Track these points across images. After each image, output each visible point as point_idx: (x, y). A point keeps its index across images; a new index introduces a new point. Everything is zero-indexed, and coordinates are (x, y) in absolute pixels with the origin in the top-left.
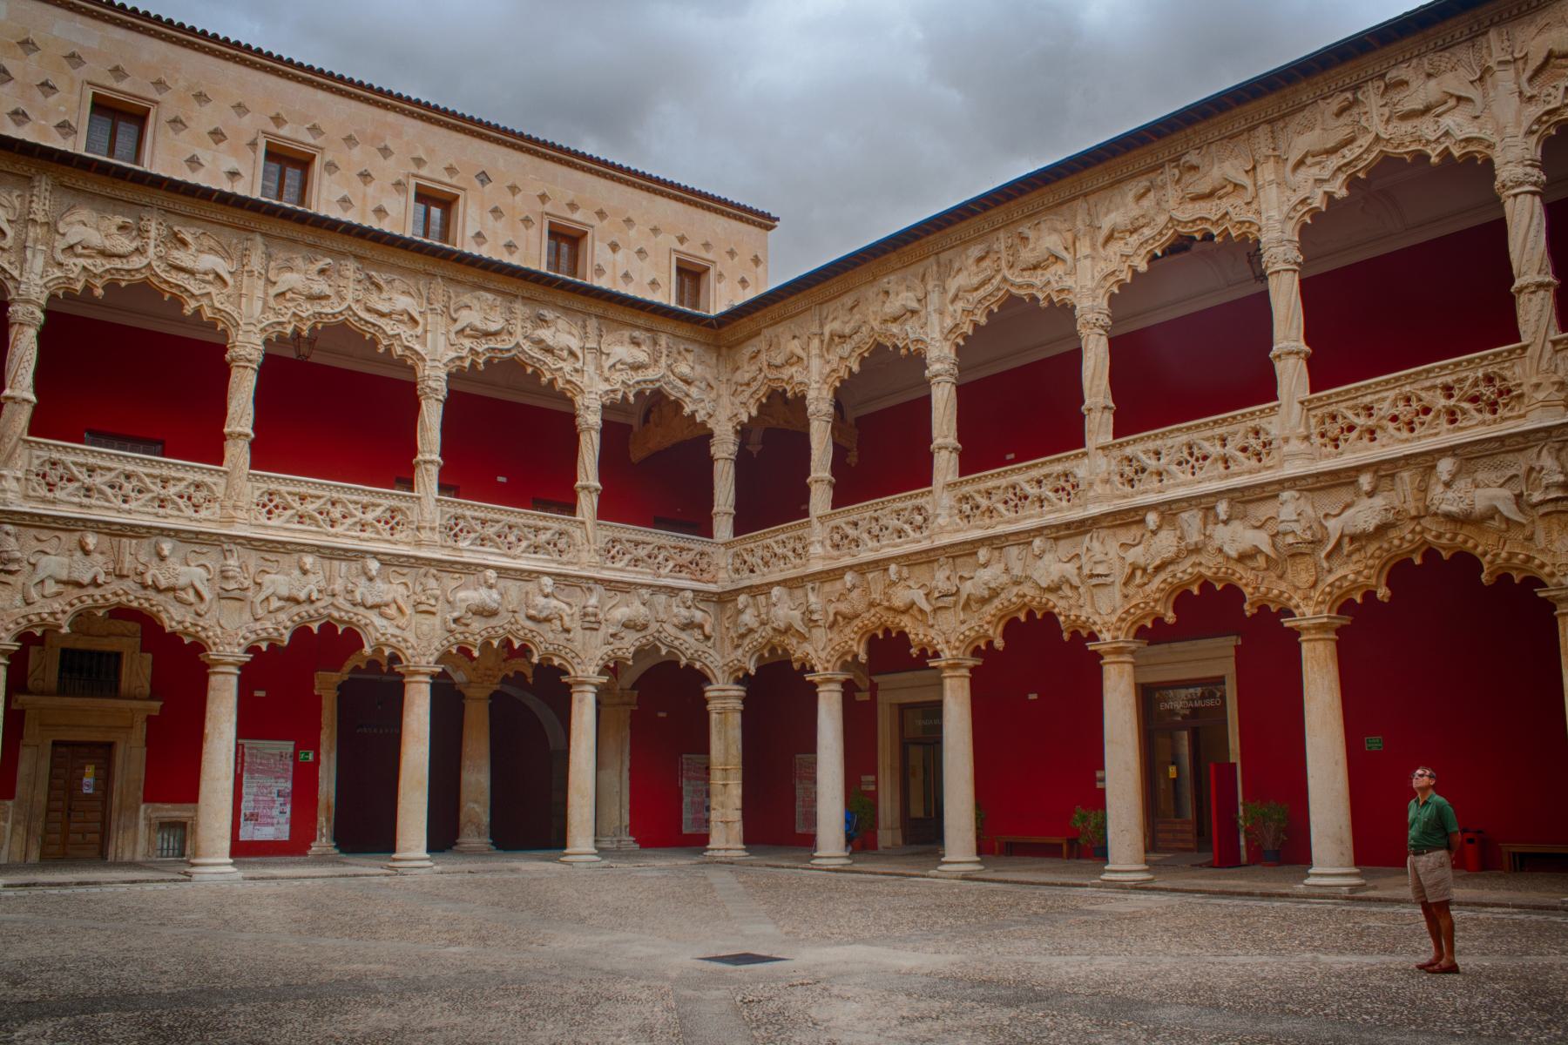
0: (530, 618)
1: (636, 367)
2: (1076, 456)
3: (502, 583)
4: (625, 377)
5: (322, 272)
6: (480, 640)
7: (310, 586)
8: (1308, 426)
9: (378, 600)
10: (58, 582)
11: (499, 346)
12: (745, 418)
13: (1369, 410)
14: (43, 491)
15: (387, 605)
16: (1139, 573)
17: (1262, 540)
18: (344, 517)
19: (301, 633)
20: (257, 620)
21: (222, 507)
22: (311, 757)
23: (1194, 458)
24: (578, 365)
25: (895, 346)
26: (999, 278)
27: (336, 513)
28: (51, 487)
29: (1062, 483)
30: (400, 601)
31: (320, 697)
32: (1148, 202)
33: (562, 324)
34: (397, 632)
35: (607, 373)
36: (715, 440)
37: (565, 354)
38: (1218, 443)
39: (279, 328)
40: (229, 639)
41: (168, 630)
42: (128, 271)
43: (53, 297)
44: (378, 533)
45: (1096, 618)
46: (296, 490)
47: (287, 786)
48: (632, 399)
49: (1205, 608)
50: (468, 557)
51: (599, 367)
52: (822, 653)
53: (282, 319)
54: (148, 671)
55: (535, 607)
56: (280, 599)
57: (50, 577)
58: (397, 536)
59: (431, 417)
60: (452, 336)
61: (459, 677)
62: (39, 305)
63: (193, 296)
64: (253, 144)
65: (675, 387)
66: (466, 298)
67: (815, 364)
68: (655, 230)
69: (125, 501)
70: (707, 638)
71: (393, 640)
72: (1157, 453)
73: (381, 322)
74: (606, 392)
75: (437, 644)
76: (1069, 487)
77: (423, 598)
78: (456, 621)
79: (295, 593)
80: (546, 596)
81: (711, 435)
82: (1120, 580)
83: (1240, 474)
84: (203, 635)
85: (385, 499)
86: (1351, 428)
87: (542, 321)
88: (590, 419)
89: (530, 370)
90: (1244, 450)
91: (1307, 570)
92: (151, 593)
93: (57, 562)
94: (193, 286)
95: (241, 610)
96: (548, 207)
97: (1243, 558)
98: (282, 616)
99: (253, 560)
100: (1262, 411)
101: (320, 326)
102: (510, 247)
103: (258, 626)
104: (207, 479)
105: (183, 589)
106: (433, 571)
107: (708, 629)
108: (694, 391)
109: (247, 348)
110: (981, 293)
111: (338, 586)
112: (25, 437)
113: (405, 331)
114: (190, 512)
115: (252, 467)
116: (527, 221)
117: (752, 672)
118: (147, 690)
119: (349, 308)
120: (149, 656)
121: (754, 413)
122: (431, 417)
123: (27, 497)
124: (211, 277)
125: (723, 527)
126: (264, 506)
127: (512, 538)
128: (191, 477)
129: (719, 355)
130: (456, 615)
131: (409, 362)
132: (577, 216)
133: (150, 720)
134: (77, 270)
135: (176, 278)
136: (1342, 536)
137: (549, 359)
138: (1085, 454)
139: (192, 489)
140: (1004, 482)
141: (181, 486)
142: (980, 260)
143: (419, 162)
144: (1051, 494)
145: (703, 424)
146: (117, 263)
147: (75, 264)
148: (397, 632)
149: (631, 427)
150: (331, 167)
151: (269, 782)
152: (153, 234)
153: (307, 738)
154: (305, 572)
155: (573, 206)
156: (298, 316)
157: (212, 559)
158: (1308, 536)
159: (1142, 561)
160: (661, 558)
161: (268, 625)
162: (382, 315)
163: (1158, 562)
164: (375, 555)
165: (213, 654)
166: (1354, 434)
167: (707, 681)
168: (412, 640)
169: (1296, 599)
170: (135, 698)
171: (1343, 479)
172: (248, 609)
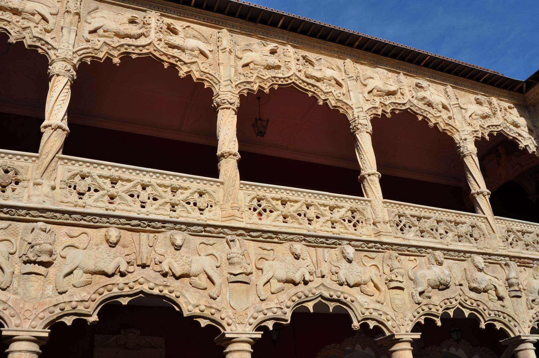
0: (472, 289)
3: (446, 262)
4: (480, 123)
5: (273, 52)
6: (440, 312)
18: (318, 217)
21: (222, 209)
24: (450, 114)
27: (311, 213)
30: (375, 280)
34: (378, 306)
37: (440, 107)
39: (248, 86)
41: (186, 314)
42: (137, 47)
44: (346, 228)
46: (278, 196)
48: (487, 138)
51: (464, 117)
53: (249, 80)
55: (475, 280)
56: (279, 281)
60: (366, 95)
63: (185, 63)
65: (511, 130)
69: (143, 207)
71: (375, 315)
73: (318, 84)
75: (410, 315)
77: (393, 277)
78: (421, 293)
80: (480, 270)
84: (217, 317)
85: (346, 203)
88: (469, 148)
89: (420, 118)
92: (170, 280)
94: (185, 57)
95: (248, 291)
98: (283, 297)
99: (253, 248)
101: (276, 87)
103: (264, 306)
106: (395, 254)
111: (325, 269)
115: (241, 179)
124: (197, 53)
126: (255, 210)
129: (529, 112)
130: (420, 289)
131: (341, 111)
134: (100, 44)
135: (171, 52)
139: (196, 195)
141: (187, 193)
148: (378, 306)
152: (153, 25)
154: (297, 257)
156: (261, 80)
157: (220, 248)
161: (272, 305)
162: (318, 80)
172: (253, 291)
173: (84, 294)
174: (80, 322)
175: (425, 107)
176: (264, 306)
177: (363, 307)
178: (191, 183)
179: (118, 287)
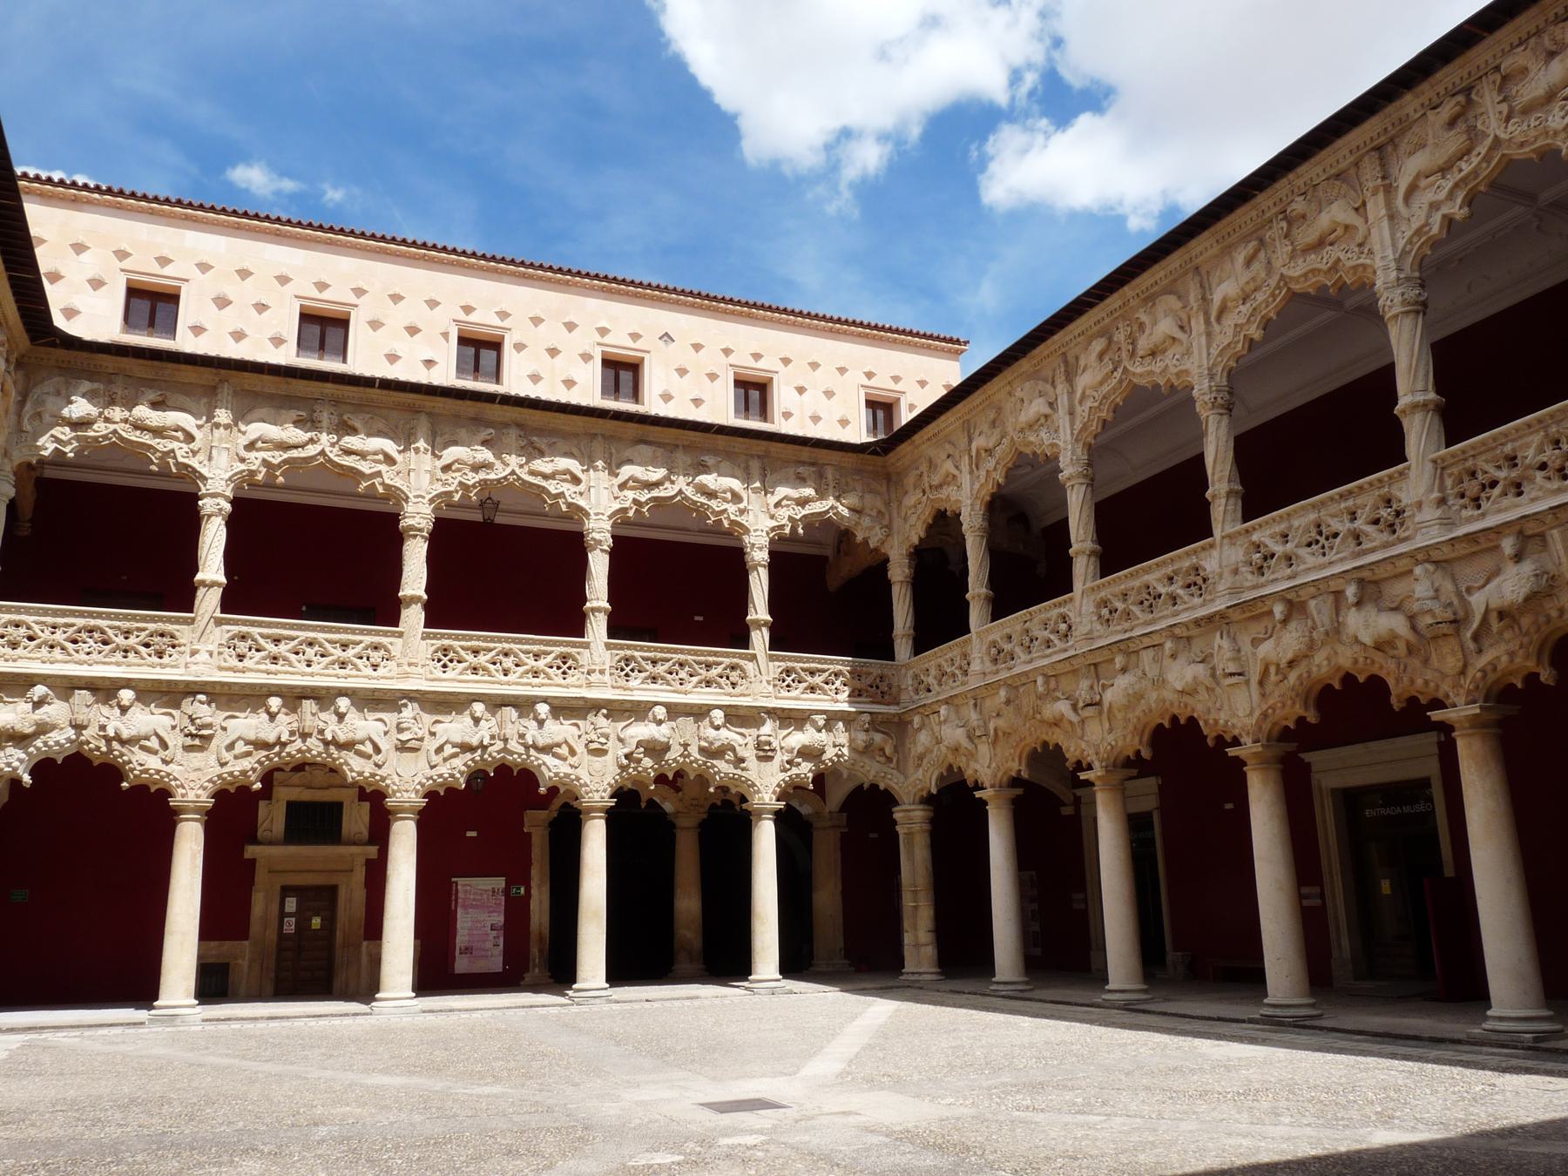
1: (803, 502)
2: (1203, 549)
4: (791, 513)
7: (483, 733)
8: (1442, 488)
9: (549, 741)
10: (248, 743)
11: (662, 494)
12: (916, 541)
13: (1512, 460)
14: (234, 662)
15: (559, 745)
16: (1272, 670)
17: (1396, 624)
19: (476, 775)
20: (432, 767)
21: (399, 665)
22: (522, 890)
23: (1321, 538)
25: (1035, 453)
26: (1120, 370)
27: (508, 662)
28: (241, 657)
29: (1192, 578)
31: (529, 834)
32: (1257, 266)
33: (726, 465)
36: (890, 565)
37: (729, 495)
38: (1346, 517)
40: (407, 786)
43: (237, 488)
45: (1235, 721)
47: (499, 919)
49: (1353, 707)
50: (638, 696)
52: (989, 768)
54: (367, 819)
57: (240, 738)
58: (569, 680)
59: (599, 566)
61: (668, 807)
64: (445, 335)
66: (628, 453)
67: (965, 479)
68: (842, 370)
70: (889, 760)
72: (1285, 537)
74: (773, 529)
76: (1200, 581)
77: (594, 737)
78: (627, 756)
79: (467, 739)
80: (717, 728)
81: (887, 560)
82: (1254, 679)
83: (1373, 550)
85: (556, 645)
86: (1494, 484)
87: (704, 469)
88: (759, 556)
90: (1376, 522)
91: (1453, 653)
93: (249, 724)
94: (365, 467)
96: (732, 359)
97: (1379, 646)
100: (1390, 477)
102: (697, 402)
104: (384, 640)
105: (362, 743)
107: (888, 751)
108: (866, 522)
109: (418, 516)
110: (1106, 388)
112: (218, 614)
113: (567, 489)
114: (369, 671)
116: (713, 377)
117: (934, 791)
118: (365, 834)
119: (513, 472)
121: (923, 535)
123: (221, 669)
124: (381, 457)
125: (903, 648)
128: (368, 639)
130: (626, 751)
132: (761, 364)
134: (257, 463)
136: (1487, 611)
137: (713, 503)
138: (1212, 546)
140: (1137, 583)
141: (359, 649)
142: (1101, 356)
143: (603, 331)
144: (1180, 592)
145: (876, 550)
146: (294, 453)
147: (256, 458)
148: (569, 770)
149: (826, 558)
150: (519, 347)
151: (483, 916)
152: (325, 423)
153: (518, 874)
155: (757, 356)
158: (1449, 615)
159: (1273, 657)
160: (838, 683)
162: (546, 477)
163: (1290, 656)
164: (545, 700)
165: (390, 802)
166: (1497, 491)
167: (897, 804)
168: (585, 778)
169: (1445, 687)
170: (354, 844)
171: (1481, 544)
173: (246, 764)
174: (244, 790)
175: (703, 500)
176: (434, 773)
177: (551, 768)
178: (364, 635)
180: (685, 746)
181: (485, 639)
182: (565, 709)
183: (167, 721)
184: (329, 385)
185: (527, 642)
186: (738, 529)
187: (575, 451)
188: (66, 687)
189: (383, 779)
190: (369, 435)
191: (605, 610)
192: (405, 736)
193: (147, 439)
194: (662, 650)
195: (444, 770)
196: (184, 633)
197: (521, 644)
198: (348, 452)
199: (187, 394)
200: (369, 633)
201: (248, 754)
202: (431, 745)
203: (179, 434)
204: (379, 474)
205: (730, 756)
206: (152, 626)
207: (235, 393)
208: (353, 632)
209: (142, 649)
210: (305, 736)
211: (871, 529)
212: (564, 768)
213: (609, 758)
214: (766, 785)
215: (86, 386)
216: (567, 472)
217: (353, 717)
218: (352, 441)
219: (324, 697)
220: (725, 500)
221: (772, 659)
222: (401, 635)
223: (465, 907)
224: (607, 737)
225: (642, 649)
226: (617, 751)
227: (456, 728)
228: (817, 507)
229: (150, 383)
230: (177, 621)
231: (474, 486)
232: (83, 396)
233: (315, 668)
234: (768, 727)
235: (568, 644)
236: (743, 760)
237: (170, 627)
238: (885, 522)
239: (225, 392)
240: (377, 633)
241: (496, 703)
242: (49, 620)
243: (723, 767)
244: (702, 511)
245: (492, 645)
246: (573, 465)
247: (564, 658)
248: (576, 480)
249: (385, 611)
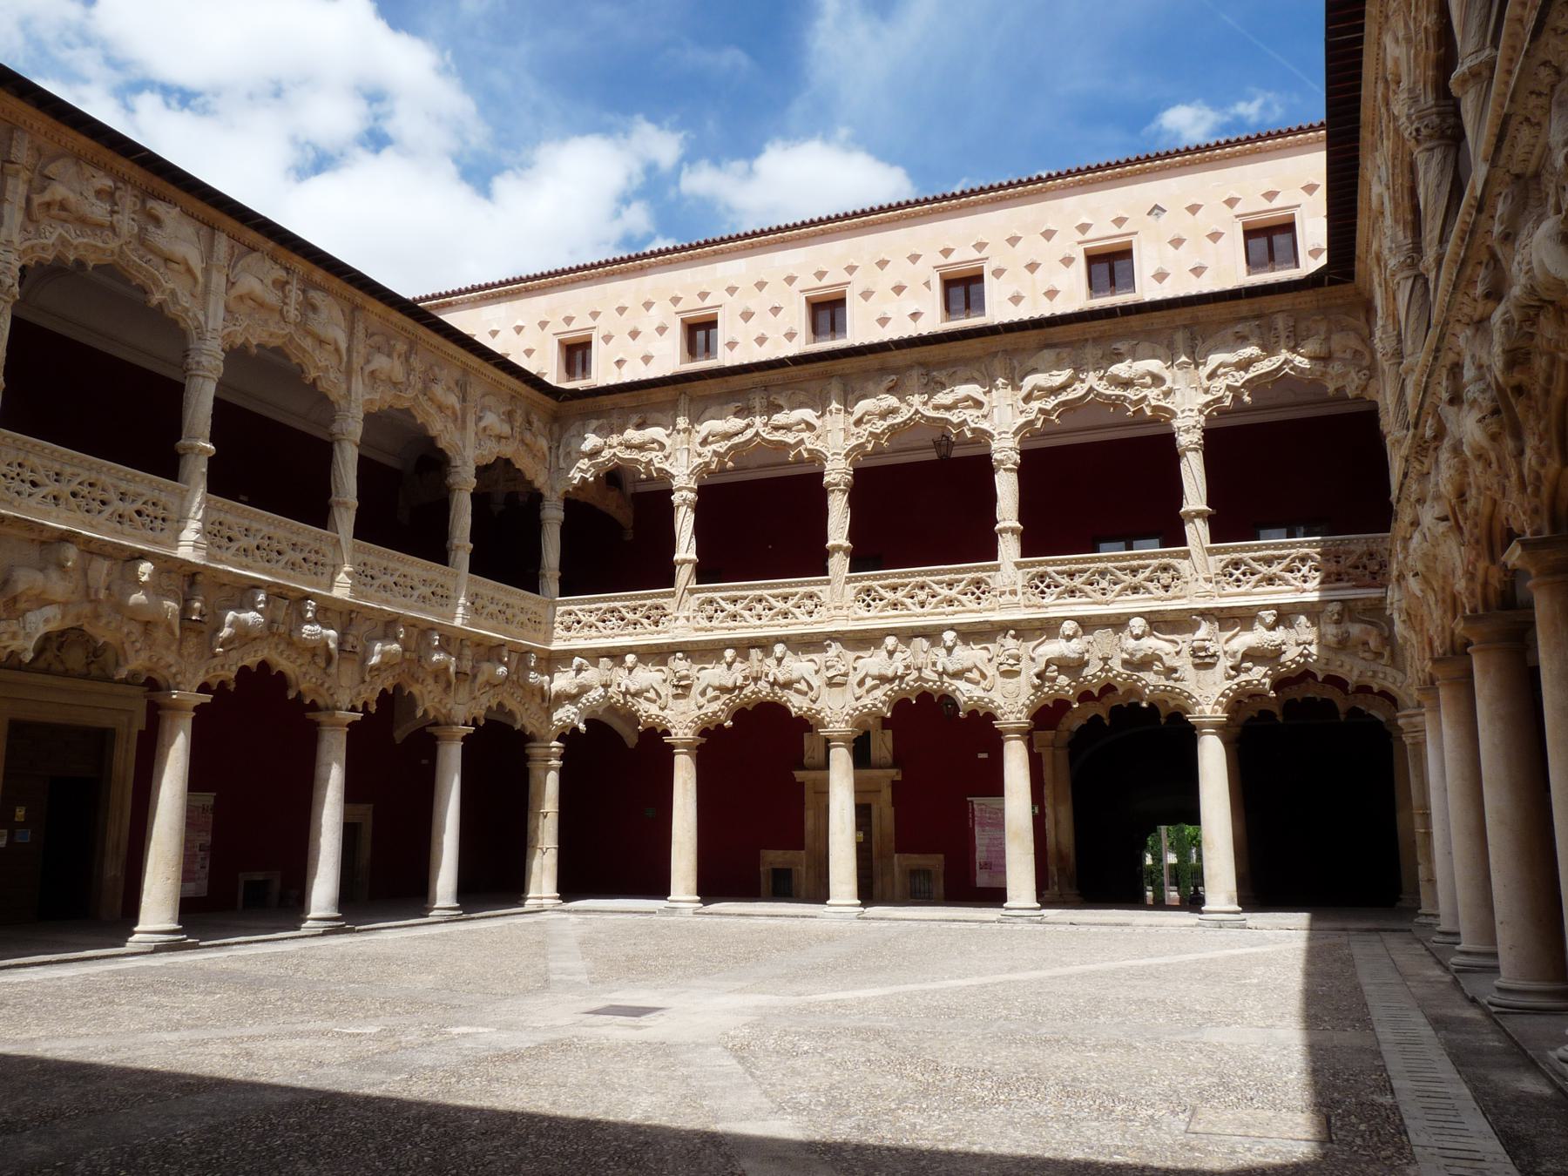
10: (715, 689)
11: (1070, 397)
15: (970, 670)
20: (857, 699)
28: (710, 618)
35: (1206, 383)
37: (1148, 380)
43: (699, 479)
50: (1053, 613)
54: (890, 744)
58: (984, 604)
59: (1007, 488)
62: (691, 490)
66: (1031, 363)
74: (1207, 405)
78: (1039, 676)
80: (1137, 638)
85: (967, 572)
87: (1118, 357)
93: (715, 674)
94: (790, 438)
104: (815, 589)
108: (1336, 368)
109: (837, 472)
113: (970, 415)
118: (890, 759)
119: (917, 412)
120: (890, 732)
122: (1007, 488)
127: (1104, 584)
130: (1036, 670)
133: (894, 784)
135: (778, 436)
137: (1131, 394)
143: (1084, 228)
145: (1358, 398)
146: (736, 440)
148: (982, 694)
150: (998, 273)
155: (1270, 195)
162: (948, 408)
164: (952, 627)
168: (999, 700)
173: (715, 706)
175: (1119, 392)
178: (799, 587)
179: (738, 699)
180: (1105, 660)
181: (900, 576)
182: (973, 634)
183: (660, 676)
184: (756, 374)
185: (938, 573)
186: (1163, 416)
187: (976, 374)
188: (594, 656)
189: (819, 712)
190: (792, 409)
191: (1013, 531)
192: (831, 673)
193: (635, 455)
194: (1077, 562)
195: (867, 701)
196: (670, 604)
197: (933, 576)
198: (776, 428)
199: (661, 411)
200: (803, 584)
201: (716, 698)
202: (854, 679)
203: (655, 445)
204: (802, 442)
205: (1158, 666)
206: (649, 602)
207: (692, 400)
208: (790, 585)
209: (645, 621)
210: (756, 679)
211: (1344, 375)
212: (977, 692)
213: (1022, 678)
214: (1207, 696)
215: (594, 423)
216: (968, 398)
217: (790, 660)
218: (780, 418)
219: (765, 645)
220: (1144, 386)
221: (1210, 552)
222: (828, 582)
223: (982, 825)
224: (1018, 658)
225: (1054, 563)
226: (1029, 671)
227: (874, 662)
228: (1265, 366)
229: (635, 409)
230: (664, 596)
231: (883, 433)
232: (594, 432)
233: (764, 621)
234: (1204, 630)
235: (977, 569)
236: (1175, 670)
237: (660, 601)
238: (1365, 363)
239: (683, 403)
240: (809, 584)
241: (907, 635)
242: (586, 607)
243: (1151, 679)
244: (1117, 404)
245: (906, 581)
246: (973, 390)
247: (978, 583)
248: (979, 404)
249: (813, 562)
